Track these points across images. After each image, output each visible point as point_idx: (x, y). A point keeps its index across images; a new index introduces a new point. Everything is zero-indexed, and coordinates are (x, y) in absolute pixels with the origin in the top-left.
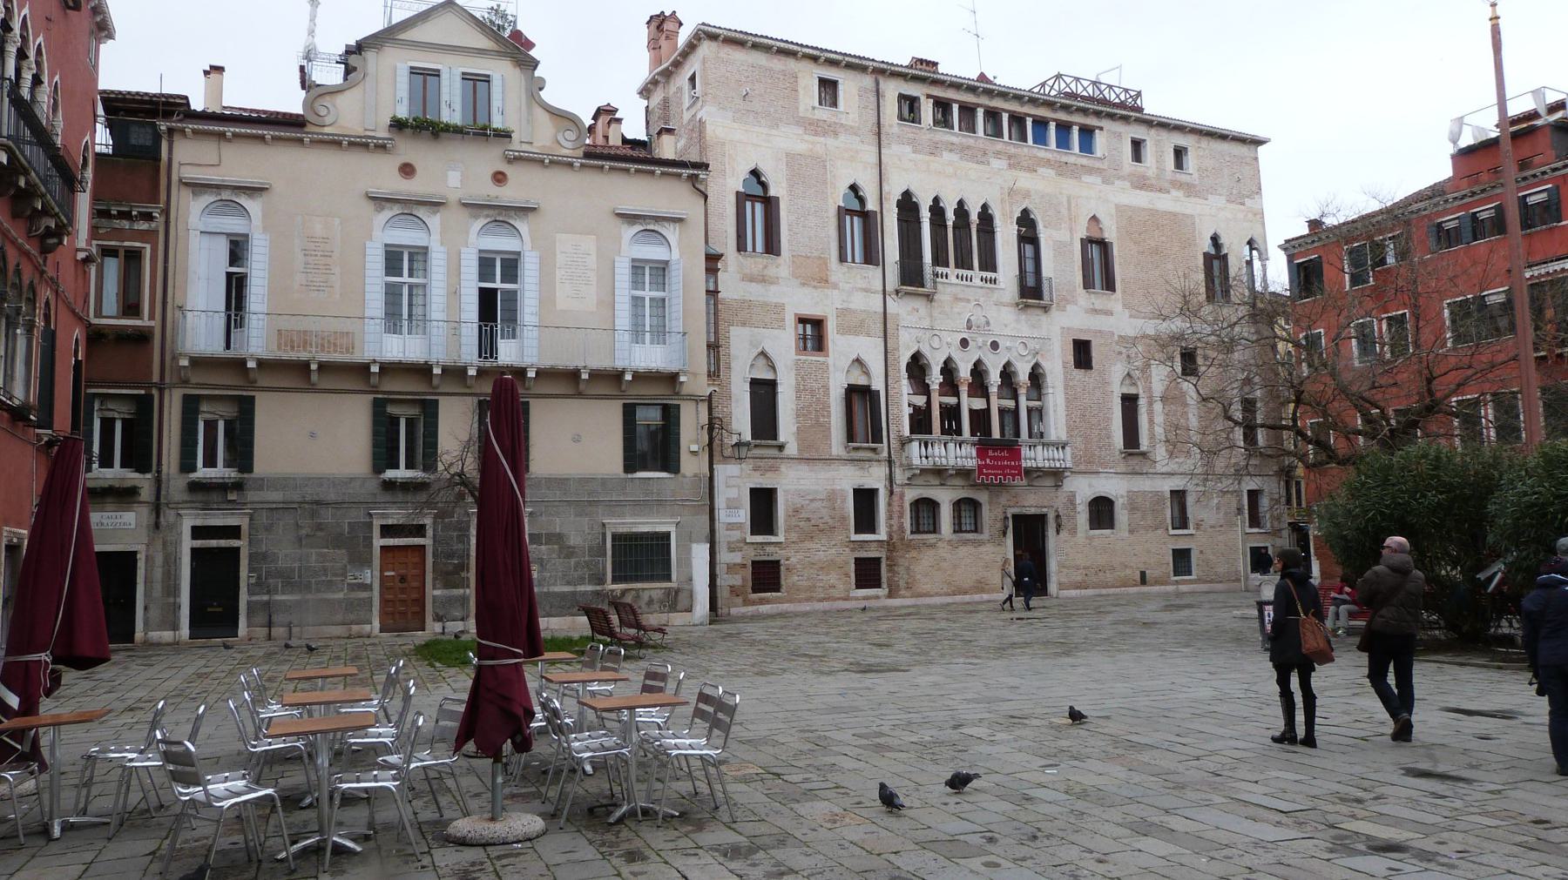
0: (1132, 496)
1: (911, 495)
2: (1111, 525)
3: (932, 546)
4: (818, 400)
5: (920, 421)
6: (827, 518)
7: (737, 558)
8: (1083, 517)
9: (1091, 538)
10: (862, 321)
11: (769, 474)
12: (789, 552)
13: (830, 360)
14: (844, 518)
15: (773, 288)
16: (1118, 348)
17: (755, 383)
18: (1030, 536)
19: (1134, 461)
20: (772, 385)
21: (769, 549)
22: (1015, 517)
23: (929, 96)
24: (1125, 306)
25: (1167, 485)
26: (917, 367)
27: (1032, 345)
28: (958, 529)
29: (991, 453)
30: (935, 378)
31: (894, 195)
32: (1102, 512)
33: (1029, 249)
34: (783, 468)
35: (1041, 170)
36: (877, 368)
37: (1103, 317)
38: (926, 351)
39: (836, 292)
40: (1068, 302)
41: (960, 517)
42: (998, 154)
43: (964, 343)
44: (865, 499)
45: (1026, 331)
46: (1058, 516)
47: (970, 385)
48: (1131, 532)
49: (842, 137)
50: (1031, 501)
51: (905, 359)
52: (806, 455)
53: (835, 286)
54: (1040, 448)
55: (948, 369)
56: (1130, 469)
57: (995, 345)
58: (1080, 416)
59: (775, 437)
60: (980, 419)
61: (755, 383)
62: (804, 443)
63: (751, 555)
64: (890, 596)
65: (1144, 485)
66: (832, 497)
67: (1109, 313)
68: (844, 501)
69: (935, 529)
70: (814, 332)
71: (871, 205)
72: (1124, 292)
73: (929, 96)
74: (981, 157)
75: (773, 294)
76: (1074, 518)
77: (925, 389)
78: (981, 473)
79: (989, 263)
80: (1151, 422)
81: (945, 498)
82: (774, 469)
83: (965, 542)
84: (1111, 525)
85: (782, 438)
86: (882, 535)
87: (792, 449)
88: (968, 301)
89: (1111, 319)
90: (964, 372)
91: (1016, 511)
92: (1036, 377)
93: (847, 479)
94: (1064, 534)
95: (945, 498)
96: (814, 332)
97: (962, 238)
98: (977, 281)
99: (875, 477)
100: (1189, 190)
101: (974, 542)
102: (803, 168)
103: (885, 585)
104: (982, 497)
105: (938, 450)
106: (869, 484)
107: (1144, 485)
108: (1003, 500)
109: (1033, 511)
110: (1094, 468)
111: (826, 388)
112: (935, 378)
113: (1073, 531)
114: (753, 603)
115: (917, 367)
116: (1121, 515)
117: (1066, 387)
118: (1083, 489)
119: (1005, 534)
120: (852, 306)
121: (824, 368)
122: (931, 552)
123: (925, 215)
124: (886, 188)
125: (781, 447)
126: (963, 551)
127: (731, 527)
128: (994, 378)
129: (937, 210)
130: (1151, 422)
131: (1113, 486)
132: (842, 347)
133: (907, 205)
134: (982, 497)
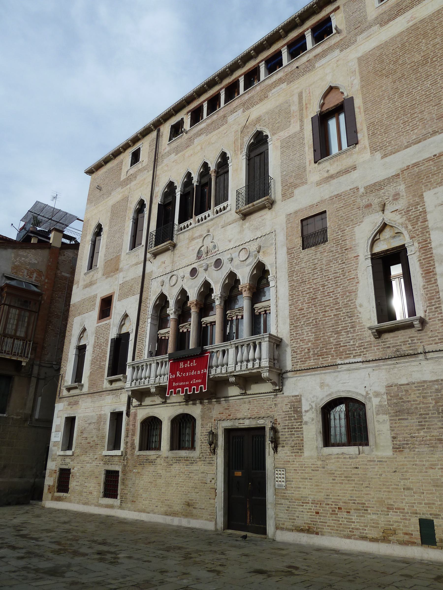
3: (152, 462)
6: (95, 438)
8: (312, 429)
9: (325, 459)
10: (132, 286)
14: (103, 437)
16: (365, 202)
18: (246, 452)
22: (228, 432)
24: (374, 149)
32: (348, 421)
43: (194, 272)
45: (249, 235)
48: (398, 449)
49: (138, 177)
52: (92, 391)
56: (390, 352)
64: (121, 507)
76: (300, 430)
83: (178, 460)
89: (355, 175)
91: (228, 424)
103: (119, 497)
104: (195, 410)
109: (247, 423)
110: (330, 360)
113: (299, 448)
116: (379, 426)
117: (291, 274)
118: (310, 390)
119: (214, 452)
120: (127, 279)
122: (151, 468)
126: (176, 468)
131: (362, 381)
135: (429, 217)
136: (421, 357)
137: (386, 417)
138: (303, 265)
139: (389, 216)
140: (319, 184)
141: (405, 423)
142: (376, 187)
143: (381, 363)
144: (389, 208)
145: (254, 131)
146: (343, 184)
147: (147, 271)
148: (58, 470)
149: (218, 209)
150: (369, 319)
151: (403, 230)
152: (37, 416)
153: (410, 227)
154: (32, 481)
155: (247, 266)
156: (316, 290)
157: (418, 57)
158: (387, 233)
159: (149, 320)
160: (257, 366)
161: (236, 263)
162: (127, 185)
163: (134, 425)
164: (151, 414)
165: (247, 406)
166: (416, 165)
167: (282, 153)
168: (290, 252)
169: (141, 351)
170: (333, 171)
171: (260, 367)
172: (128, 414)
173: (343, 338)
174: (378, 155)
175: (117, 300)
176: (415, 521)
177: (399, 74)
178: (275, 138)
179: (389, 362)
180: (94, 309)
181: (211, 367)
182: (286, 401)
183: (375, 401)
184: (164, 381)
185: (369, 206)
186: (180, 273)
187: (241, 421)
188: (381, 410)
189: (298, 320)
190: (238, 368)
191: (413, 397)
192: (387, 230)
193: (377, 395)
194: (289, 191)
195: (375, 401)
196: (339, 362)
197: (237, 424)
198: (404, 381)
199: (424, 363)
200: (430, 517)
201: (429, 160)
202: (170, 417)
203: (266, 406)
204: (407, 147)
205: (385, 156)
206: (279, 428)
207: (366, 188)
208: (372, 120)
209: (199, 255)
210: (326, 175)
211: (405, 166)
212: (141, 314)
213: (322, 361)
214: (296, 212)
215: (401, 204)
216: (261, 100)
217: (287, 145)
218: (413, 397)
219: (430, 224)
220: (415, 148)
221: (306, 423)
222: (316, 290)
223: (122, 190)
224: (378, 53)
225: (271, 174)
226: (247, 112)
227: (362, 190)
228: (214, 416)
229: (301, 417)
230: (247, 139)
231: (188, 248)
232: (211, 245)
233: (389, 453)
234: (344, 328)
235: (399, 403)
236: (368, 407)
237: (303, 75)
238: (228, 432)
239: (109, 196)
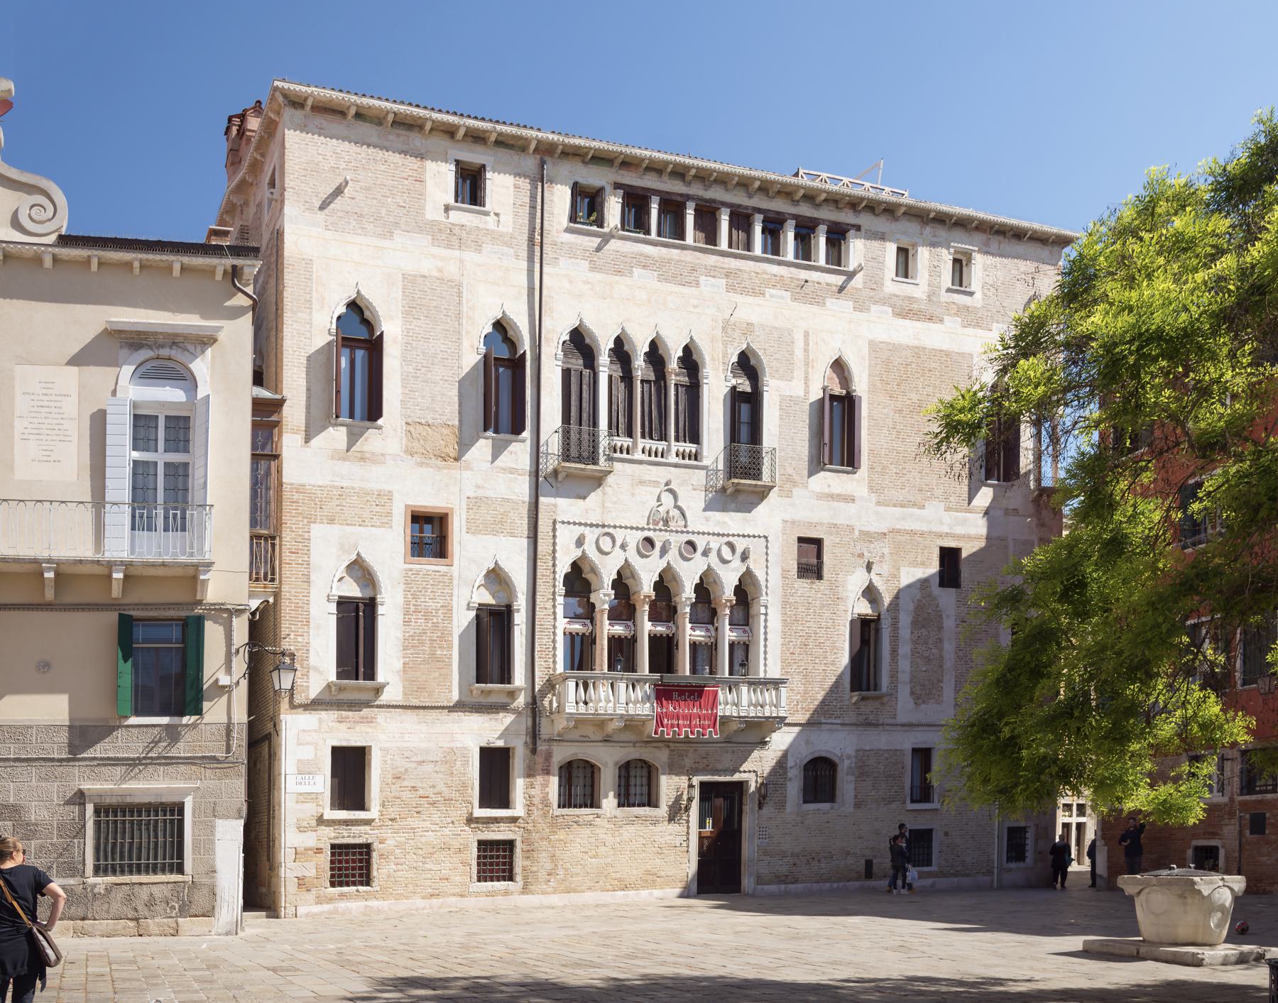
0: (862, 756)
2: (831, 798)
4: (435, 625)
5: (580, 653)
13: (455, 570)
17: (344, 604)
19: (868, 707)
20: (370, 606)
25: (908, 742)
26: (578, 582)
27: (741, 545)
30: (604, 597)
33: (745, 409)
35: (769, 291)
37: (842, 505)
38: (592, 554)
41: (628, 786)
47: (653, 605)
48: (858, 805)
51: (563, 567)
54: (744, 689)
55: (622, 585)
59: (371, 675)
60: (664, 651)
61: (344, 604)
65: (880, 740)
67: (850, 499)
70: (430, 533)
71: (526, 346)
72: (871, 468)
74: (687, 278)
76: (783, 786)
77: (589, 613)
78: (660, 723)
80: (894, 651)
84: (831, 798)
85: (381, 677)
89: (852, 509)
90: (646, 587)
92: (745, 594)
96: (430, 533)
97: (655, 393)
101: (645, 819)
105: (603, 690)
107: (880, 740)
111: (448, 609)
112: (604, 597)
113: (781, 805)
114: (330, 900)
115: (578, 582)
116: (846, 785)
117: (785, 603)
120: (488, 493)
123: (604, 360)
125: (378, 690)
128: (688, 594)
129: (621, 352)
130: (894, 651)
132: (473, 552)
133: (580, 342)
142: (868, 537)
146: (845, 514)
149: (681, 450)
166: (898, 531)
174: (874, 497)
175: (464, 529)
176: (863, 862)
183: (847, 763)
193: (849, 757)
195: (847, 763)
198: (867, 748)
204: (895, 506)
205: (878, 503)
210: (827, 491)
220: (899, 509)
229: (785, 773)
236: (839, 768)
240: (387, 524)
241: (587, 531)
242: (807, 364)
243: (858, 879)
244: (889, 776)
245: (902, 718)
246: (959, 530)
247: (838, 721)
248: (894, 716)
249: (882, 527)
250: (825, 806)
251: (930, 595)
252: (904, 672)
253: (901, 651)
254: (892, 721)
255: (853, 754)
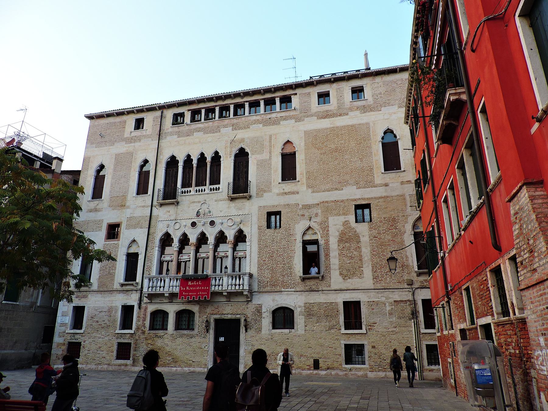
1: (152, 308)
6: (106, 321)
7: (61, 340)
8: (267, 321)
10: (140, 221)
11: (82, 299)
12: (85, 338)
13: (120, 242)
14: (115, 321)
15: (99, 213)
16: (301, 213)
21: (77, 336)
22: (216, 321)
23: (189, 110)
24: (308, 187)
25: (340, 299)
28: (178, 327)
29: (190, 283)
31: (165, 158)
32: (283, 318)
34: (89, 296)
36: (142, 242)
39: (128, 210)
40: (265, 191)
42: (225, 126)
43: (194, 224)
44: (127, 310)
45: (234, 212)
46: (245, 320)
50: (228, 311)
52: (101, 289)
53: (128, 207)
56: (307, 288)
57: (212, 223)
58: (266, 255)
62: (101, 284)
63: (69, 338)
66: (110, 310)
68: (116, 312)
69: (164, 327)
73: (189, 110)
74: (217, 130)
75: (98, 216)
76: (260, 321)
79: (216, 180)
81: (172, 309)
82: (85, 297)
83: (181, 336)
86: (131, 332)
87: (95, 287)
88: (199, 202)
89: (297, 196)
91: (217, 317)
92: (240, 237)
93: (120, 300)
94: (250, 332)
95: (172, 309)
96: (113, 231)
97: (203, 171)
98: (207, 191)
99: (133, 300)
100: (365, 109)
102: (122, 160)
103: (131, 359)
104: (195, 309)
106: (129, 303)
108: (209, 310)
109: (229, 317)
113: (259, 330)
116: (299, 320)
117: (260, 240)
118: (269, 302)
119: (208, 331)
120: (135, 215)
121: (117, 247)
124: (160, 157)
127: (63, 324)
134: (195, 309)
135: (330, 229)
136: (320, 292)
137: (303, 317)
138: (267, 237)
139: (313, 224)
140: (278, 195)
141: (311, 320)
142: (307, 207)
143: (303, 293)
144: (313, 220)
145: (240, 147)
146: (292, 199)
147: (153, 214)
148: (66, 343)
149: (212, 188)
150: (299, 271)
151: (318, 232)
152: (38, 304)
153: (321, 232)
154: (34, 351)
155: (233, 229)
156: (273, 252)
157: (333, 146)
158: (310, 232)
159: (157, 248)
160: (241, 288)
161: (225, 226)
162: (131, 143)
163: (145, 315)
164: (159, 308)
165: (230, 307)
166: (327, 202)
167: (258, 168)
168: (260, 228)
169: (150, 268)
170: (286, 191)
171: (243, 289)
172: (140, 307)
173: (286, 279)
174: (310, 190)
176: (312, 360)
177: (323, 151)
178: (254, 156)
179: (306, 293)
180: (100, 230)
181: (212, 285)
182: (254, 306)
184: (177, 290)
185: (303, 215)
186: (184, 223)
187: (226, 315)
188: (301, 313)
189: (262, 266)
190: (230, 288)
191: (315, 309)
192: (310, 230)
194: (261, 192)
195: (299, 309)
196: (283, 290)
197: (223, 317)
199: (321, 295)
200: (318, 358)
201: (332, 202)
202: (175, 312)
203: (241, 308)
205: (313, 192)
206: (248, 320)
207: (303, 205)
208: (309, 170)
209: (198, 214)
210: (282, 191)
211: (322, 201)
212: (149, 243)
213: (274, 287)
214: (264, 207)
215: (319, 219)
216: (245, 128)
217: (261, 164)
218: (315, 309)
219: (330, 233)
220: (327, 193)
221: (264, 318)
222: (273, 252)
223: (126, 145)
224: (315, 134)
225: (250, 179)
226: (235, 132)
227: (301, 206)
228: (208, 312)
230: (235, 150)
231: (189, 207)
232: (207, 211)
233: (303, 332)
234: (287, 274)
235: (310, 312)
237: (273, 125)
238: (216, 321)
239: (112, 145)
240: (100, 230)
241: (170, 222)
242: (271, 146)
243: (309, 369)
244: (327, 316)
245: (333, 287)
246: (366, 196)
247: (293, 290)
248: (330, 286)
249: (316, 202)
250: (287, 331)
251: (350, 227)
252: (335, 264)
253: (332, 255)
254: (328, 289)
255: (303, 305)
